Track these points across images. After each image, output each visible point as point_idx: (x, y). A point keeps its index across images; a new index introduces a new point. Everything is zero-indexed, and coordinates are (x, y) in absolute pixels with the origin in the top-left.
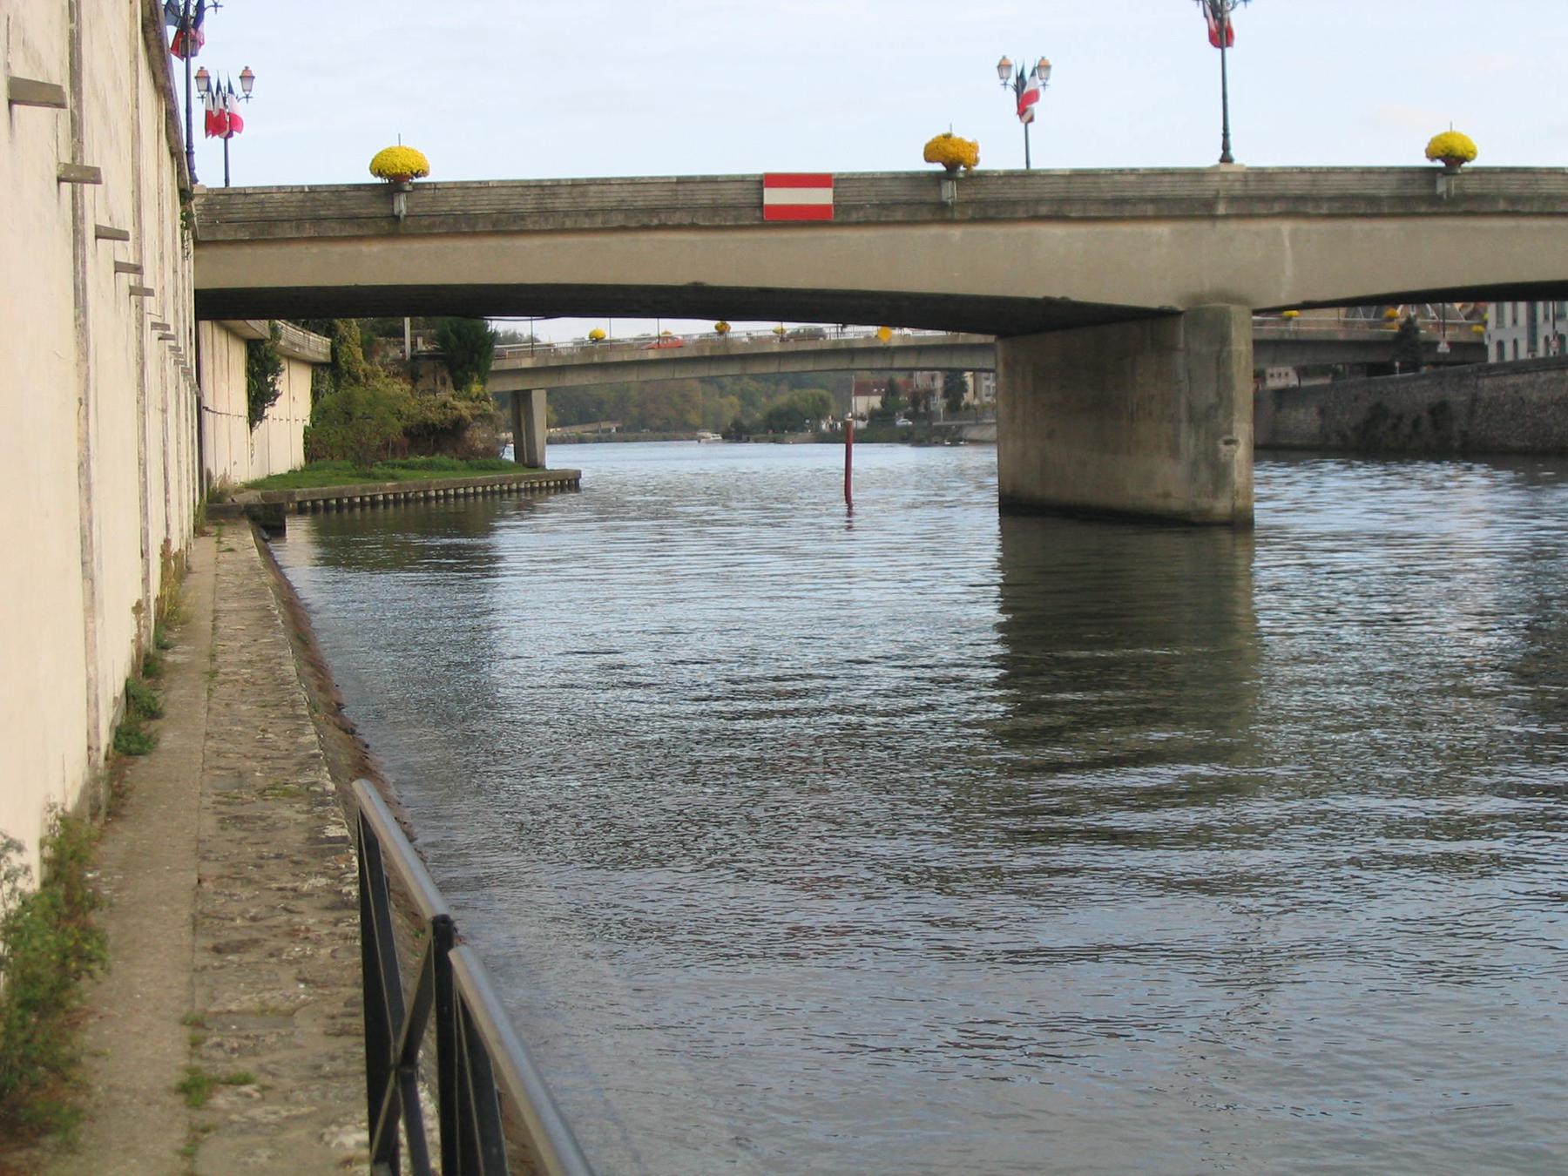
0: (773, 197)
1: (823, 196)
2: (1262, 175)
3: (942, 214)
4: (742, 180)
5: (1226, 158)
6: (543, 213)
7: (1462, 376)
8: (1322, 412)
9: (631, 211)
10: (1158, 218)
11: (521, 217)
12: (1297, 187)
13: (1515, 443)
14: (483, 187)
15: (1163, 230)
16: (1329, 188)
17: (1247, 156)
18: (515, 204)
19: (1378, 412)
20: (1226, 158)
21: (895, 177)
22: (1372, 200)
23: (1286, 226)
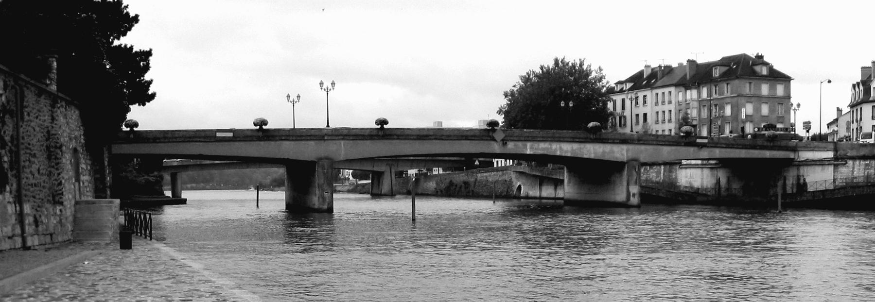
0: (218, 135)
1: (231, 135)
2: (336, 130)
3: (259, 139)
4: (212, 130)
5: (328, 126)
6: (165, 138)
7: (473, 173)
8: (437, 184)
9: (186, 137)
10: (311, 140)
11: (159, 138)
12: (345, 132)
13: (485, 194)
14: (151, 131)
15: (312, 143)
16: (353, 133)
17: (332, 125)
18: (158, 136)
19: (451, 183)
20: (328, 126)
21: (248, 130)
22: (363, 136)
23: (342, 142)
